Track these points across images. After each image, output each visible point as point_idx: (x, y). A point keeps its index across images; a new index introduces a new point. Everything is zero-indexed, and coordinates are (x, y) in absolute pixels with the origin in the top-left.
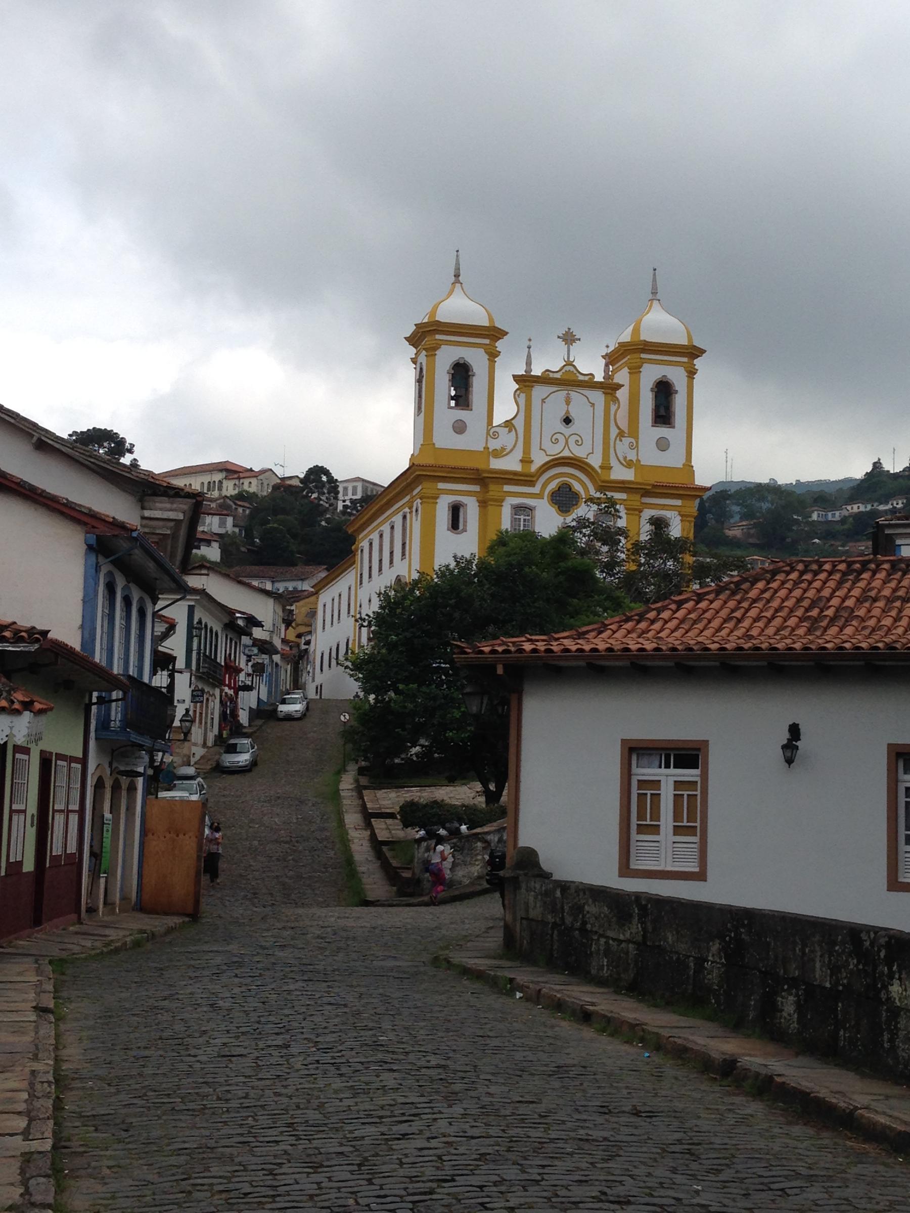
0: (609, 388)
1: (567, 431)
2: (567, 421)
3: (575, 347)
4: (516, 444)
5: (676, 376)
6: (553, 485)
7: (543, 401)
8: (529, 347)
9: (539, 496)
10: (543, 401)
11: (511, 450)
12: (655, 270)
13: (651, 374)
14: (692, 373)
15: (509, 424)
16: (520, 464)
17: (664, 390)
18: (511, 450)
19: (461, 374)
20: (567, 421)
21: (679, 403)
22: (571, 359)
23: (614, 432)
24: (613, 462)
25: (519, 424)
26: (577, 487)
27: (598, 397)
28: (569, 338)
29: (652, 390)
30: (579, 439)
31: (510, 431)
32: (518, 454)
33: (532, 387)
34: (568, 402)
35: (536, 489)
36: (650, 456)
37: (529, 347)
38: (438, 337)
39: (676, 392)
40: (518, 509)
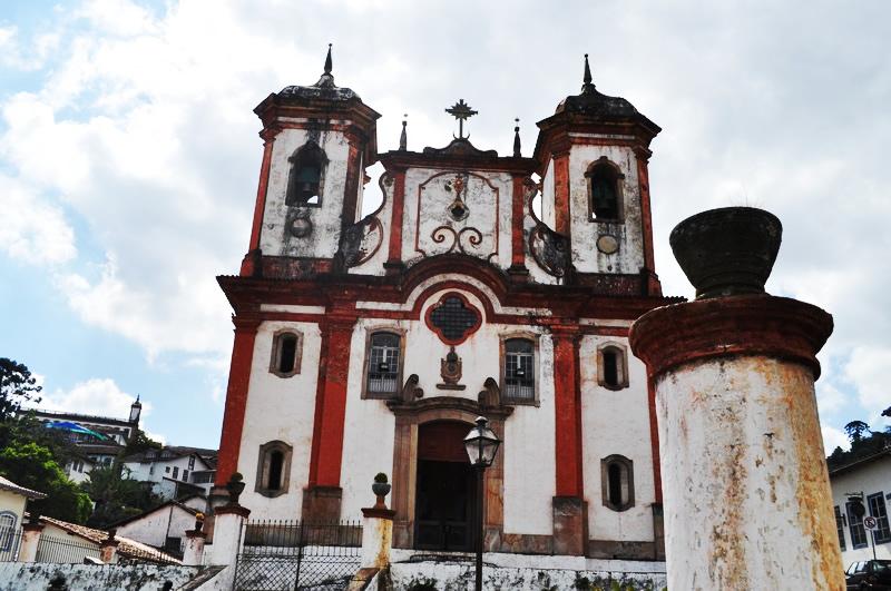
0: (518, 167)
1: (458, 226)
2: (459, 211)
3: (469, 122)
4: (378, 247)
5: (617, 155)
6: (435, 299)
7: (421, 187)
8: (405, 124)
9: (413, 315)
10: (421, 187)
11: (373, 255)
12: (586, 56)
13: (583, 157)
14: (643, 156)
15: (372, 220)
16: (384, 271)
17: (603, 176)
18: (373, 255)
19: (309, 165)
20: (459, 211)
21: (628, 196)
22: (465, 136)
23: (529, 224)
24: (530, 264)
25: (386, 218)
26: (473, 300)
27: (505, 182)
28: (461, 111)
29: (586, 175)
30: (476, 235)
31: (371, 229)
32: (384, 255)
33: (407, 168)
34: (461, 187)
35: (409, 306)
36: (587, 261)
37: (405, 124)
38: (281, 119)
39: (623, 177)
40: (377, 338)
